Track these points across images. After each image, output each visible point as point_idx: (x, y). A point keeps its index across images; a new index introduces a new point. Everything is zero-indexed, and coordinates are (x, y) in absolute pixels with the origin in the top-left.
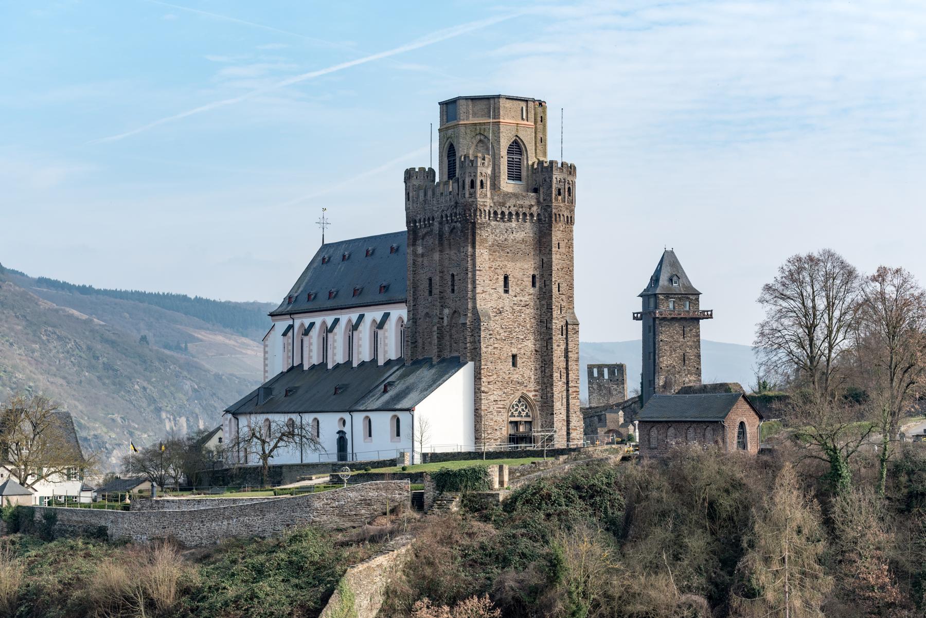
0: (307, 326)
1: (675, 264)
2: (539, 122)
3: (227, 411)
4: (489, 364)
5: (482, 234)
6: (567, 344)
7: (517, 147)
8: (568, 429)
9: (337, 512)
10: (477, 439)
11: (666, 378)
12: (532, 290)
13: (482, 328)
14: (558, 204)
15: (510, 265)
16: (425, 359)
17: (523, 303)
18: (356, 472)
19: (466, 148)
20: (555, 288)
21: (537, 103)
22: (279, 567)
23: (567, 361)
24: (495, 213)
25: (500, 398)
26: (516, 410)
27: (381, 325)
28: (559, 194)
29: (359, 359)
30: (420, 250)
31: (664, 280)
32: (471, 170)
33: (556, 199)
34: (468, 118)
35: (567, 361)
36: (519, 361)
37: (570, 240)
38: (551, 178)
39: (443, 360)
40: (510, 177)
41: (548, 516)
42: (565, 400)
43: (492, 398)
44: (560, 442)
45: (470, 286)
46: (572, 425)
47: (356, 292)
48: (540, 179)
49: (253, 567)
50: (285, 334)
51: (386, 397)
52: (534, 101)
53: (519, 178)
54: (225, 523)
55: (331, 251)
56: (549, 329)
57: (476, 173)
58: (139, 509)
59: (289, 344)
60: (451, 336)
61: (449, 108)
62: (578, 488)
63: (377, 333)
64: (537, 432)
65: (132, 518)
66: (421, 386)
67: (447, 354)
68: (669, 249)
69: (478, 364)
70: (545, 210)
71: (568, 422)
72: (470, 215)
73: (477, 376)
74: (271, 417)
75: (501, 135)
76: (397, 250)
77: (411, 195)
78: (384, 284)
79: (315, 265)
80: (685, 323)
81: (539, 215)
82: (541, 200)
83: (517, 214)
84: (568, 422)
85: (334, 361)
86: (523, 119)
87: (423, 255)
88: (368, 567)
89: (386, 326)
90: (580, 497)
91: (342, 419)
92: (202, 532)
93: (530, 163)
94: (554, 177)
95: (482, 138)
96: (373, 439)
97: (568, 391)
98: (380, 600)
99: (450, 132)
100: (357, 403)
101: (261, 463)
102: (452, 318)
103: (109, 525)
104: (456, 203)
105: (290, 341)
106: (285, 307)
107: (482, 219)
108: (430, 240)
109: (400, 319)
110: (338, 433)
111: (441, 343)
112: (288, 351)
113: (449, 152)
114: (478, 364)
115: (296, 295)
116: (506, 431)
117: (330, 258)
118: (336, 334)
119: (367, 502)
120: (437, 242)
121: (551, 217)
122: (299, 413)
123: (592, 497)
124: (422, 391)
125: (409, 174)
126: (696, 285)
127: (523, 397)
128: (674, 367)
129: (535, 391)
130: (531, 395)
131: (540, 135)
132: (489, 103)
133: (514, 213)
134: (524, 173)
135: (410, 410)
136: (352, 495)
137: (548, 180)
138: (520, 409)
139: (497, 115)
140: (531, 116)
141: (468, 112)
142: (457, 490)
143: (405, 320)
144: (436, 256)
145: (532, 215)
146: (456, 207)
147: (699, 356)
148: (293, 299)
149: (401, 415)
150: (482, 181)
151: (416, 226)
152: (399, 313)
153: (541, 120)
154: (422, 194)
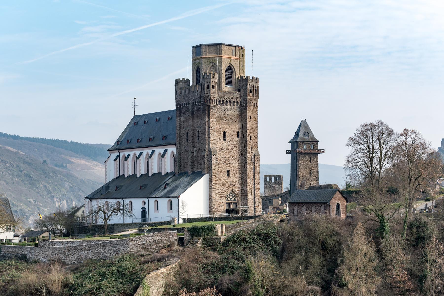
0: (126, 156)
1: (307, 126)
2: (241, 57)
3: (87, 198)
4: (216, 175)
5: (213, 111)
6: (254, 165)
7: (230, 69)
8: (254, 207)
9: (141, 247)
10: (210, 211)
11: (302, 182)
12: (237, 139)
13: (213, 157)
14: (250, 97)
15: (227, 127)
16: (184, 172)
17: (233, 145)
18: (151, 228)
19: (205, 69)
20: (248, 138)
21: (240, 47)
22: (112, 274)
23: (254, 174)
24: (220, 101)
26: (229, 197)
27: (163, 156)
28: (251, 92)
29: (152, 172)
30: (182, 119)
31: (301, 135)
32: (208, 80)
33: (249, 95)
34: (206, 54)
35: (254, 174)
36: (231, 173)
37: (256, 114)
38: (247, 84)
39: (194, 173)
40: (227, 84)
41: (245, 248)
42: (253, 193)
43: (217, 191)
44: (250, 213)
45: (207, 137)
46: (256, 204)
47: (151, 139)
48: (241, 85)
49: (100, 274)
50: (115, 160)
51: (166, 191)
52: (239, 46)
53: (231, 84)
54: (86, 252)
55: (138, 119)
56: (246, 158)
57: (210, 81)
58: (43, 246)
59: (117, 165)
60: (197, 161)
61: (197, 49)
62: (259, 235)
63: (161, 160)
64: (240, 208)
65: (39, 250)
66: (183, 185)
67: (195, 170)
68: (304, 119)
69: (210, 175)
70: (244, 100)
71: (254, 203)
72: (207, 102)
73: (210, 181)
74: (108, 200)
75: (222, 63)
76: (171, 119)
77: (178, 92)
78: (165, 135)
79: (131, 126)
80: (311, 155)
81: (241, 102)
82: (242, 95)
83: (230, 102)
84: (254, 203)
85: (140, 173)
86: (233, 55)
87: (184, 122)
88: (157, 274)
89: (166, 156)
90: (260, 239)
91: (144, 201)
92: (74, 257)
93: (237, 77)
94: (248, 84)
95: (213, 64)
96: (159, 211)
97: (254, 188)
98: (162, 289)
99: (197, 61)
100: (151, 194)
101: (104, 223)
102: (198, 152)
103: (28, 253)
104: (200, 96)
105: (118, 163)
106: (115, 146)
107: (213, 104)
108: (187, 114)
109: (173, 152)
110: (142, 208)
111: (193, 165)
112: (117, 168)
113: (197, 71)
114: (210, 175)
115: (121, 140)
116: (224, 207)
117: (138, 123)
118: (141, 160)
119: (156, 242)
120: (191, 115)
121: (247, 103)
122: (123, 198)
123: (266, 239)
124: (183, 188)
125: (177, 82)
126: (317, 137)
127: (233, 191)
128: (306, 176)
129: (238, 188)
130: (236, 190)
131: (241, 63)
132: (216, 47)
133: (229, 101)
134: (234, 82)
135: (177, 197)
136: (148, 238)
137: (245, 85)
138: (231, 197)
139: (220, 53)
140: (237, 54)
141: (206, 52)
142: (200, 236)
143: (175, 153)
144: (191, 122)
145: (237, 102)
146: (200, 98)
147: (318, 171)
148: (120, 143)
149: (172, 199)
150: (213, 85)
151: (180, 107)
152: (172, 150)
153: (242, 56)
154: (183, 91)
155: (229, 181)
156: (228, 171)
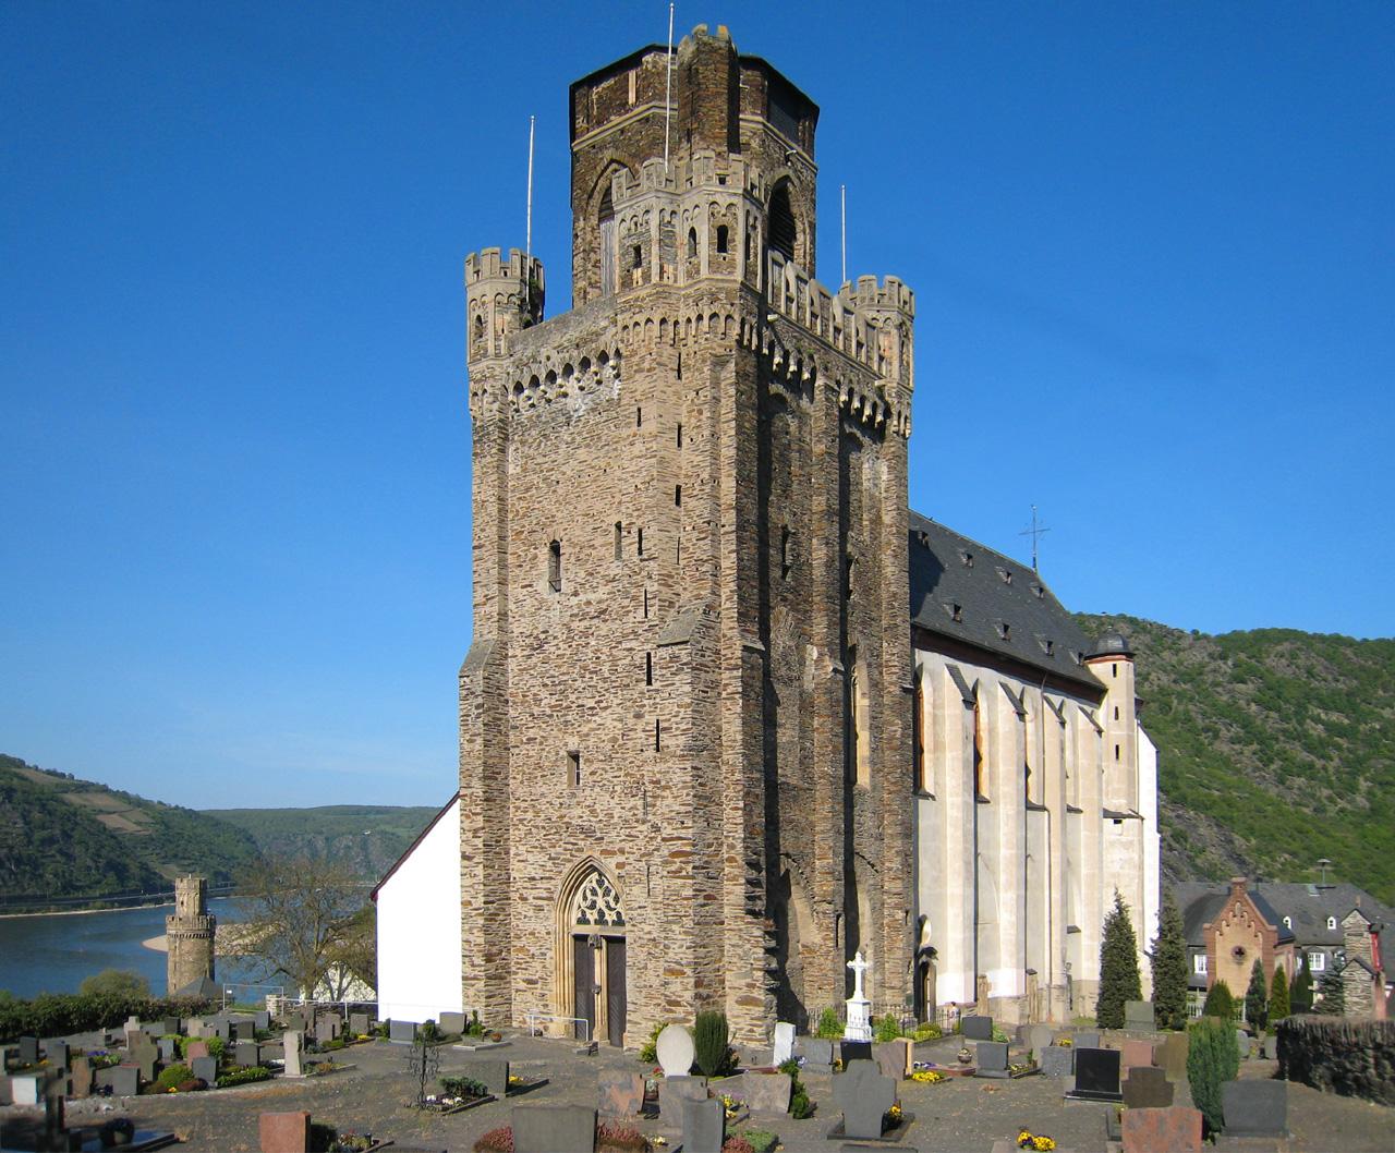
17: (592, 610)
25: (540, 873)
26: (593, 906)
155: (577, 811)
156: (575, 757)
